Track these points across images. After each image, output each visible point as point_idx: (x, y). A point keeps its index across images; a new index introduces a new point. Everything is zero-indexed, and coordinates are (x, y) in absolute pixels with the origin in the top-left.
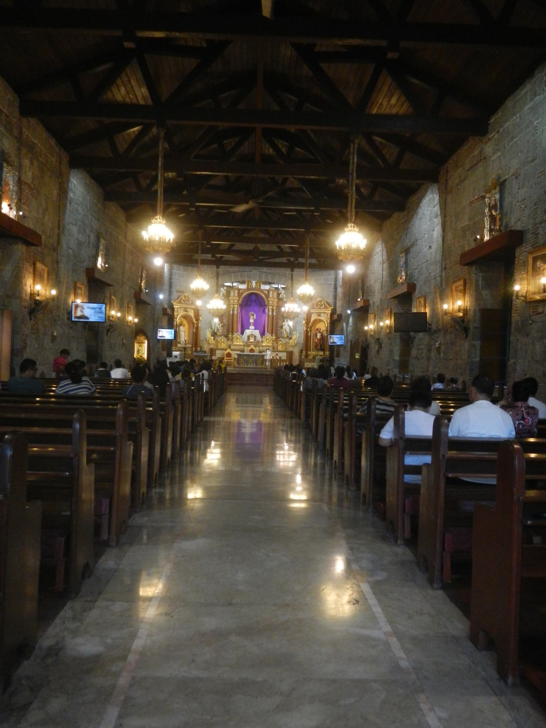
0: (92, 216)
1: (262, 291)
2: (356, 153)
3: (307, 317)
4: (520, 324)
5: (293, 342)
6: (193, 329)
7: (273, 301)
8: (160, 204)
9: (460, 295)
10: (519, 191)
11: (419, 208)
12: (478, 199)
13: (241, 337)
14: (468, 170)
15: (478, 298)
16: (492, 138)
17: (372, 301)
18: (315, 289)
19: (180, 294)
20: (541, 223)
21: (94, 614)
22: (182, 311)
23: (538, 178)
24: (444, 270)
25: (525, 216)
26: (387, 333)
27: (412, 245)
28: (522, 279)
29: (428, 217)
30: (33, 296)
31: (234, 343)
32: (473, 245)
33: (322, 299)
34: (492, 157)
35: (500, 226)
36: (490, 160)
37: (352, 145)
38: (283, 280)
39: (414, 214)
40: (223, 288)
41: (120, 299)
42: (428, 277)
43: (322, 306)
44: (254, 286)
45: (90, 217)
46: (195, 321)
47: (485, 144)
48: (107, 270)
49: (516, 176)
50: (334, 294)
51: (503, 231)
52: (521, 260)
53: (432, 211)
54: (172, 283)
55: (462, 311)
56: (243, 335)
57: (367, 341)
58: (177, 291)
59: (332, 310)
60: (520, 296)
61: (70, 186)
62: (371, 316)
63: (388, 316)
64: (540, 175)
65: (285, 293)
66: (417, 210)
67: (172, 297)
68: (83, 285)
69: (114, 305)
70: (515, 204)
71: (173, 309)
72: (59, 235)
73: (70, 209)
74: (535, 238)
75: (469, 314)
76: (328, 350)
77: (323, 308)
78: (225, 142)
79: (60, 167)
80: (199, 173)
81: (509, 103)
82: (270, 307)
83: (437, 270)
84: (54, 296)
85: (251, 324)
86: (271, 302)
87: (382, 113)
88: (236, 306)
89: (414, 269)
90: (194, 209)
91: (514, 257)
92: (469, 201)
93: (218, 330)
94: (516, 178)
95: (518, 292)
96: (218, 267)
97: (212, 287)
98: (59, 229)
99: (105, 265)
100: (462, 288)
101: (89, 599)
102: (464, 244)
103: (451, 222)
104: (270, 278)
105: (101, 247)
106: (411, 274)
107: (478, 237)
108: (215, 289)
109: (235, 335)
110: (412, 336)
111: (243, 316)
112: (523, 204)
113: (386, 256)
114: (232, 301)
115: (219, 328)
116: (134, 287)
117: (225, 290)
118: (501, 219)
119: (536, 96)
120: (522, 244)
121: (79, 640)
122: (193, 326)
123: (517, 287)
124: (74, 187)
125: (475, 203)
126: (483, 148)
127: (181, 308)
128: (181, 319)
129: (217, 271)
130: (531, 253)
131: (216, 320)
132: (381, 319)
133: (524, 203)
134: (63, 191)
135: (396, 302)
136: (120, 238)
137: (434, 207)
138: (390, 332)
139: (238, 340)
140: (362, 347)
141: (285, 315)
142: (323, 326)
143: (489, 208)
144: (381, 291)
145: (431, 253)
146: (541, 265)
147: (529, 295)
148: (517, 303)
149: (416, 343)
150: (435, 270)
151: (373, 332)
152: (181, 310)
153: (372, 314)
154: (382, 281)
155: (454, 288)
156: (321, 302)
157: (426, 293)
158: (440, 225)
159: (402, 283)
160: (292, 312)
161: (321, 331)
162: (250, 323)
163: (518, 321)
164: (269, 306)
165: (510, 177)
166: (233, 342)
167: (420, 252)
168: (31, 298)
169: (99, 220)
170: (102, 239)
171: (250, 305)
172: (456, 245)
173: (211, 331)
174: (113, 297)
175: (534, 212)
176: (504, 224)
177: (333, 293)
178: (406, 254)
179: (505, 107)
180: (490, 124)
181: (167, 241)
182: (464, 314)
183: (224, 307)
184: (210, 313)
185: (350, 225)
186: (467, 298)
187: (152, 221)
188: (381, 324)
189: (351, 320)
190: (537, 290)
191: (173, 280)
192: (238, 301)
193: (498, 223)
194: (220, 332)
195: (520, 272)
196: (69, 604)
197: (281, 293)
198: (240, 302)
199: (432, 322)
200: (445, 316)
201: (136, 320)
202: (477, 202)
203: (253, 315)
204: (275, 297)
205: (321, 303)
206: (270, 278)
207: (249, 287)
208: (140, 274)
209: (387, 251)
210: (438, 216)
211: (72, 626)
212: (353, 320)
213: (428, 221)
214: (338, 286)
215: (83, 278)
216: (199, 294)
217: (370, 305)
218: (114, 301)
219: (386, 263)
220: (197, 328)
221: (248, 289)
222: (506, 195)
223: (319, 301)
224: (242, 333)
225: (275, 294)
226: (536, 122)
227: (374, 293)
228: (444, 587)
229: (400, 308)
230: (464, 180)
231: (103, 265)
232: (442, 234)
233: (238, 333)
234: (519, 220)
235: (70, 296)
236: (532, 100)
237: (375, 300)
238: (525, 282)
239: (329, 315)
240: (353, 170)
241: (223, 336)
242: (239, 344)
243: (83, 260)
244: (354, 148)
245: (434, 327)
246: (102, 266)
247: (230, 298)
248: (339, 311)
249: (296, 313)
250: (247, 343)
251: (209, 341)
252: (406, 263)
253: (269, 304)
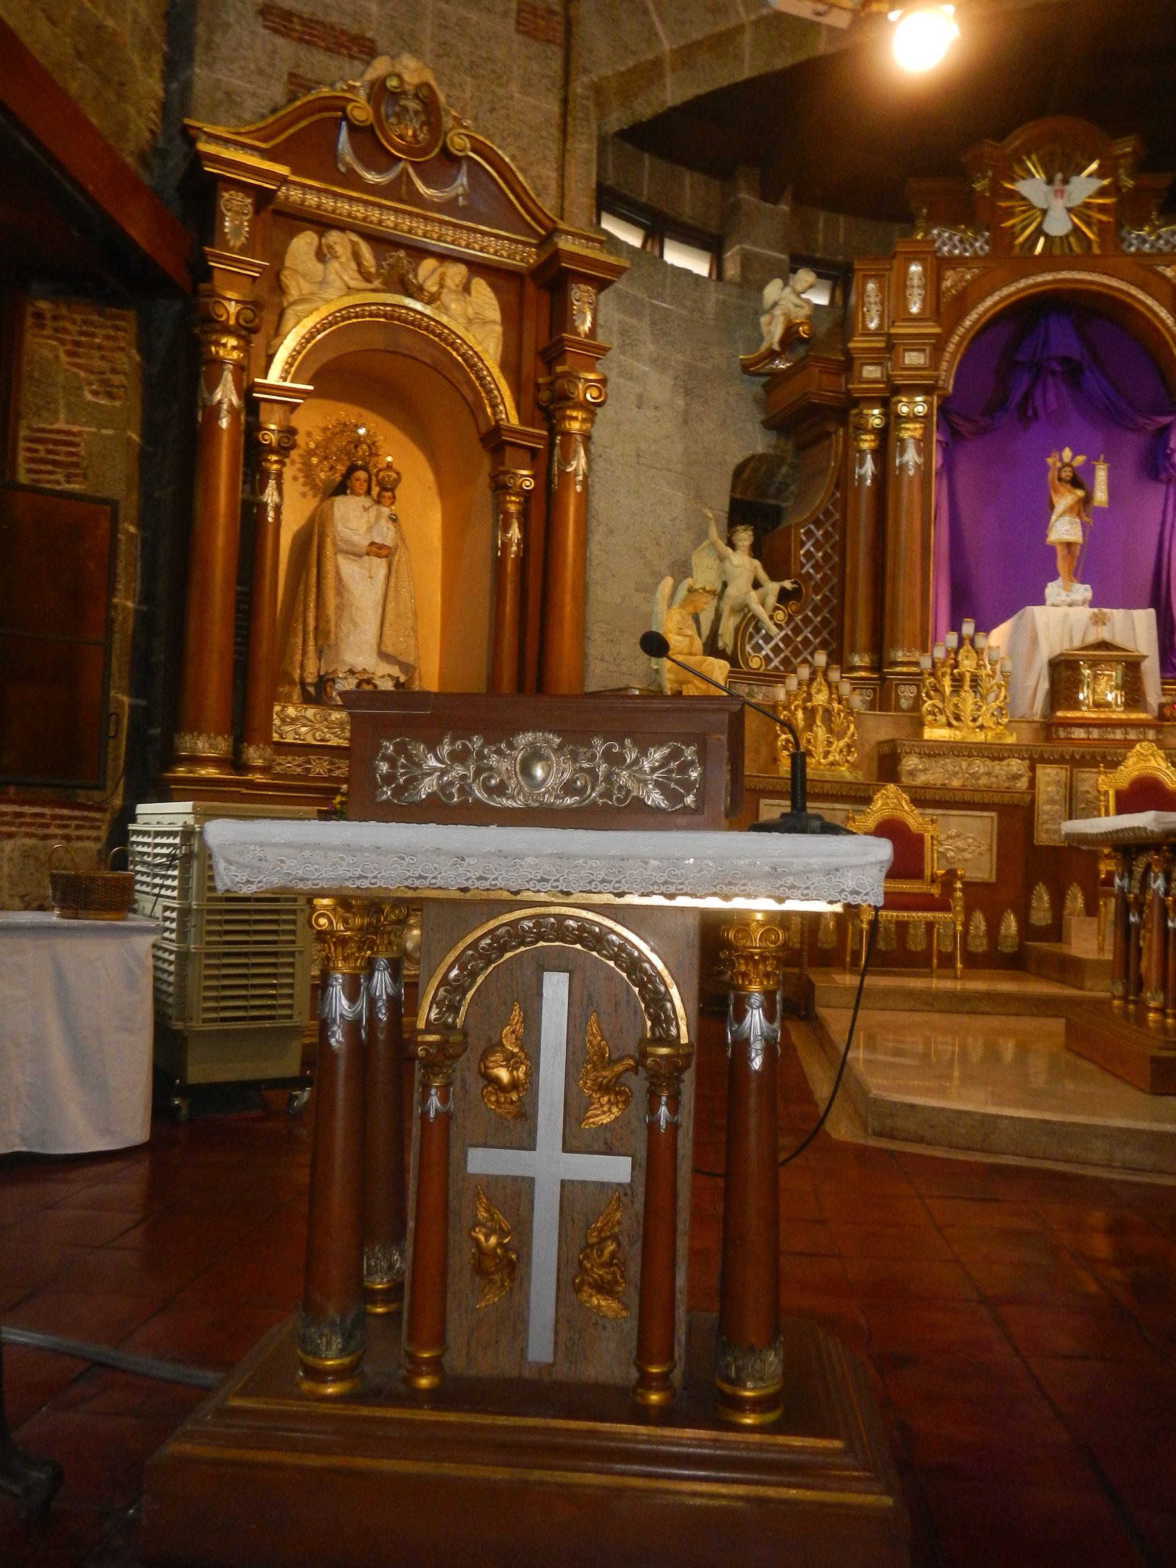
22: (341, 271)
31: (935, 733)
46: (511, 417)
85: (1061, 564)
93: (749, 624)
114: (871, 372)
115: (763, 614)
122: (500, 488)
127: (323, 224)
139: (968, 698)
152: (321, 255)
162: (1052, 549)
166: (920, 724)
171: (1027, 414)
194: (767, 650)
241: (821, 658)
242: (980, 737)
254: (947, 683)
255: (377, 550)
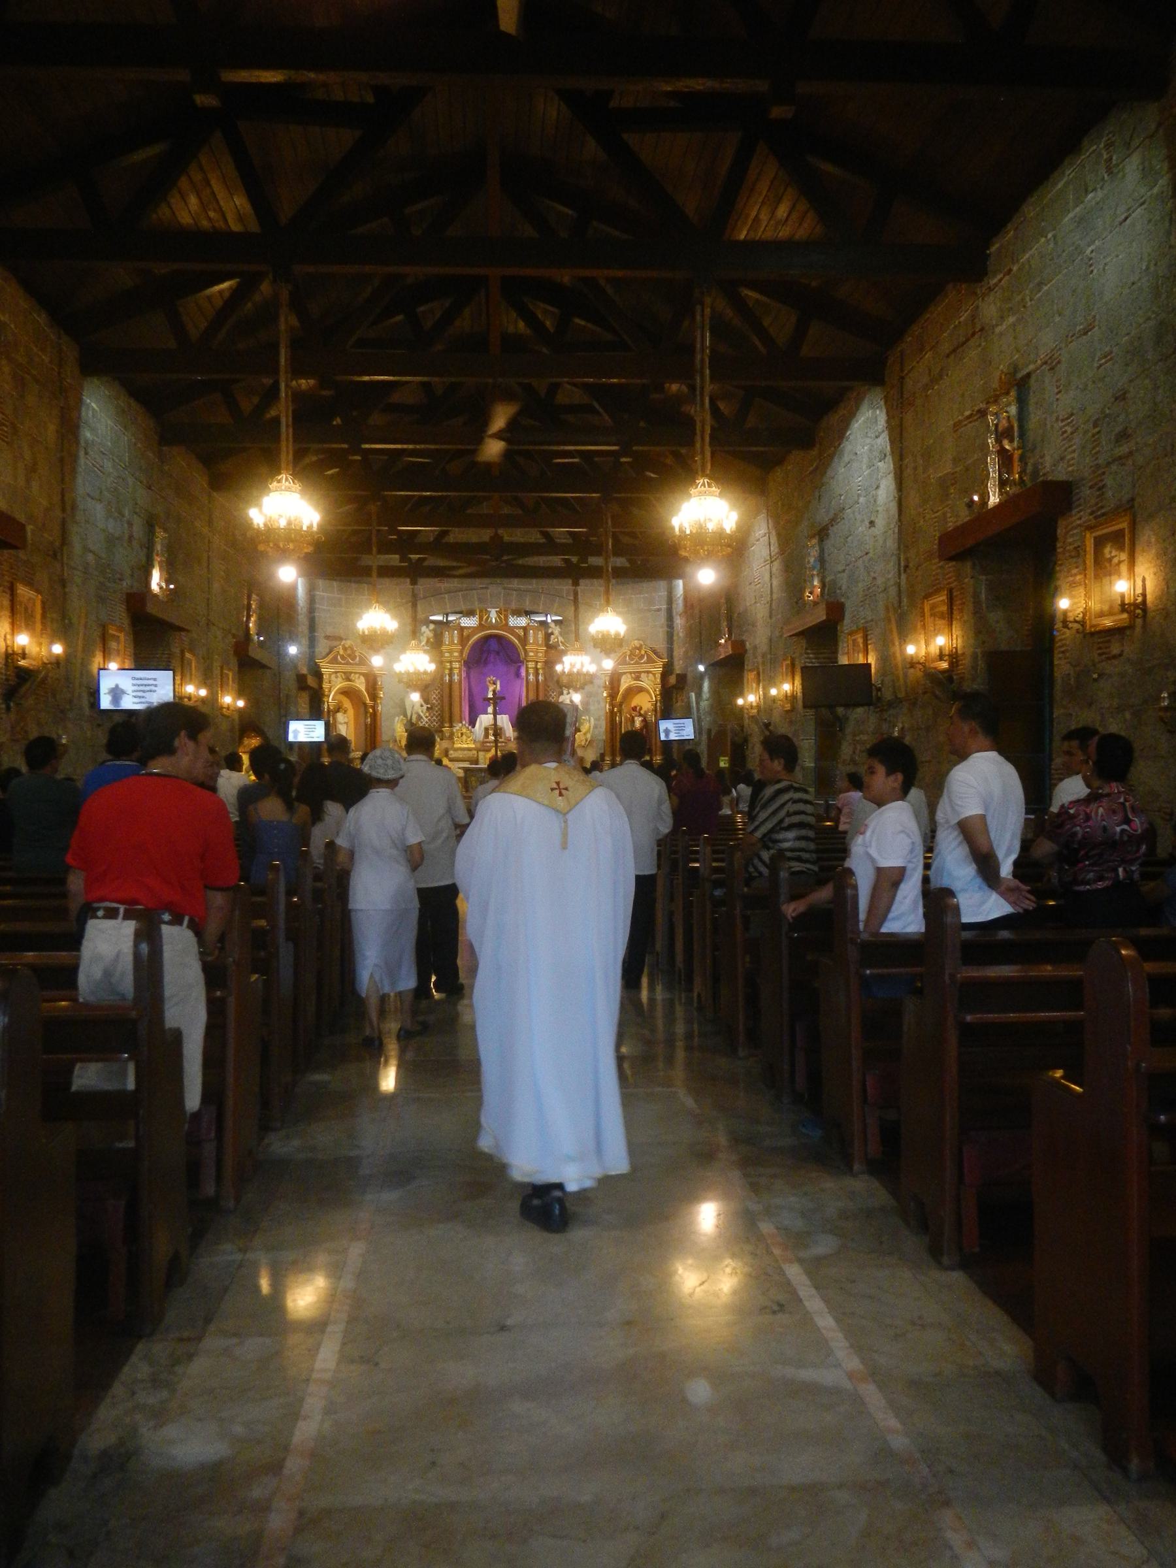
0: (136, 479)
1: (512, 630)
2: (707, 327)
3: (611, 682)
4: (1072, 681)
5: (583, 738)
6: (366, 718)
7: (537, 652)
8: (287, 447)
9: (941, 623)
10: (1058, 397)
11: (845, 440)
12: (971, 415)
13: (471, 732)
14: (948, 356)
15: (980, 629)
16: (996, 285)
17: (750, 644)
18: (626, 622)
19: (335, 643)
20: (1109, 464)
21: (198, 1367)
22: (340, 679)
23: (1099, 368)
24: (905, 571)
25: (1074, 451)
26: (786, 711)
27: (833, 521)
28: (1073, 585)
29: (865, 460)
30: (12, 659)
31: (455, 746)
32: (964, 516)
33: (641, 642)
34: (997, 325)
35: (1020, 474)
36: (993, 333)
37: (698, 308)
38: (556, 605)
39: (834, 454)
40: (428, 627)
41: (203, 658)
42: (869, 589)
43: (642, 657)
44: (494, 621)
45: (130, 480)
46: (368, 701)
47: (983, 299)
48: (173, 597)
49: (1052, 364)
50: (668, 632)
51: (1029, 484)
52: (1070, 544)
53: (872, 446)
54: (317, 619)
55: (946, 658)
56: (474, 727)
57: (742, 730)
58: (327, 637)
59: (664, 666)
60: (1071, 622)
61: (83, 414)
62: (750, 676)
63: (787, 675)
64: (1103, 361)
65: (561, 634)
66: (839, 444)
67: (317, 650)
68: (121, 631)
69: (191, 669)
70: (1052, 427)
71: (319, 676)
72: (63, 524)
73: (86, 464)
74: (1098, 496)
75: (961, 665)
76: (658, 752)
77: (644, 663)
78: (422, 309)
79: (59, 373)
80: (366, 378)
81: (1030, 210)
82: (531, 665)
83: (889, 572)
84: (58, 656)
86: (531, 654)
87: (757, 238)
88: (456, 665)
89: (839, 572)
90: (359, 458)
91: (1054, 539)
92: (951, 422)
93: (419, 717)
94: (1052, 369)
95: (1065, 613)
96: (414, 583)
97: (402, 625)
98: (64, 510)
99: (167, 585)
100: (944, 608)
101: (186, 1334)
102: (944, 514)
103: (915, 469)
104: (528, 603)
105: (158, 547)
106: (834, 582)
107: (976, 498)
108: (409, 628)
109: (458, 726)
110: (841, 715)
111: (473, 684)
112: (1068, 424)
113: (777, 545)
115: (422, 714)
116: (234, 631)
117: (430, 631)
118: (1022, 458)
119: (1087, 192)
120: (1070, 509)
121: (171, 1431)
122: (366, 712)
123: (1064, 603)
124: (93, 416)
125: (966, 425)
126: (977, 307)
127: (336, 672)
128: (337, 697)
129: (413, 589)
130: (1090, 528)
131: (415, 697)
132: (772, 681)
133: (1073, 420)
134: (70, 426)
135: (804, 643)
136: (198, 524)
137: (877, 437)
138: (793, 709)
139: (464, 737)
140: (733, 744)
141: (565, 680)
142: (646, 702)
143: (996, 435)
144: (768, 620)
145: (875, 537)
146: (1113, 555)
147: (1090, 617)
148: (1064, 636)
149: (850, 728)
150: (886, 572)
151: (756, 711)
152: (337, 677)
153: (751, 671)
154: (772, 600)
155: (927, 609)
156: (640, 649)
157: (867, 622)
158: (892, 475)
159: (815, 603)
160: (579, 673)
161: (642, 712)
163: (1069, 674)
164: (528, 661)
165: (1037, 369)
166: (454, 743)
167: (850, 535)
168: (6, 664)
169: (149, 488)
170: (160, 528)
171: (486, 663)
172: (928, 516)
173: (405, 722)
174: (188, 655)
175: (1095, 441)
176: (1029, 468)
177: (666, 629)
178: (821, 541)
179: (1022, 219)
180: (989, 255)
181: (305, 528)
182: (951, 664)
183: (432, 667)
184: (400, 681)
185: (702, 481)
186: (957, 631)
187: (270, 486)
188: (773, 692)
189: (706, 685)
190: (1106, 608)
191: (316, 614)
192: (461, 652)
193: (1017, 468)
195: (1069, 571)
196: (140, 1347)
197: (552, 634)
198: (465, 655)
199: (882, 684)
200: (912, 670)
201: (241, 704)
202: (970, 422)
203: (494, 683)
204: (540, 642)
205: (640, 651)
206: (528, 603)
207: (483, 623)
208: (246, 603)
209: (779, 535)
210: (885, 455)
211: (151, 1399)
212: (710, 687)
213: (864, 467)
214: (674, 614)
215: (121, 615)
216: (374, 641)
217: (746, 651)
218: (190, 664)
219: (778, 561)
220: (374, 715)
221: (481, 627)
222: (1031, 408)
223: (636, 648)
224: (473, 723)
225: (541, 635)
226: (1088, 252)
227: (754, 625)
228: (965, 1264)
229: (811, 656)
230: (941, 377)
231: (164, 585)
232: (897, 496)
233: (464, 723)
234: (1062, 459)
235: (94, 657)
236: (1078, 201)
237: (757, 642)
238: (1081, 591)
239: (658, 676)
240: (702, 360)
242: (466, 746)
243: (118, 576)
244: (703, 316)
245: (888, 695)
246: (161, 588)
247: (444, 648)
248: (678, 667)
249: (588, 674)
250: (484, 742)
251: (400, 741)
252: (822, 560)
253: (529, 659)
254: (460, 735)
255: (345, 723)
